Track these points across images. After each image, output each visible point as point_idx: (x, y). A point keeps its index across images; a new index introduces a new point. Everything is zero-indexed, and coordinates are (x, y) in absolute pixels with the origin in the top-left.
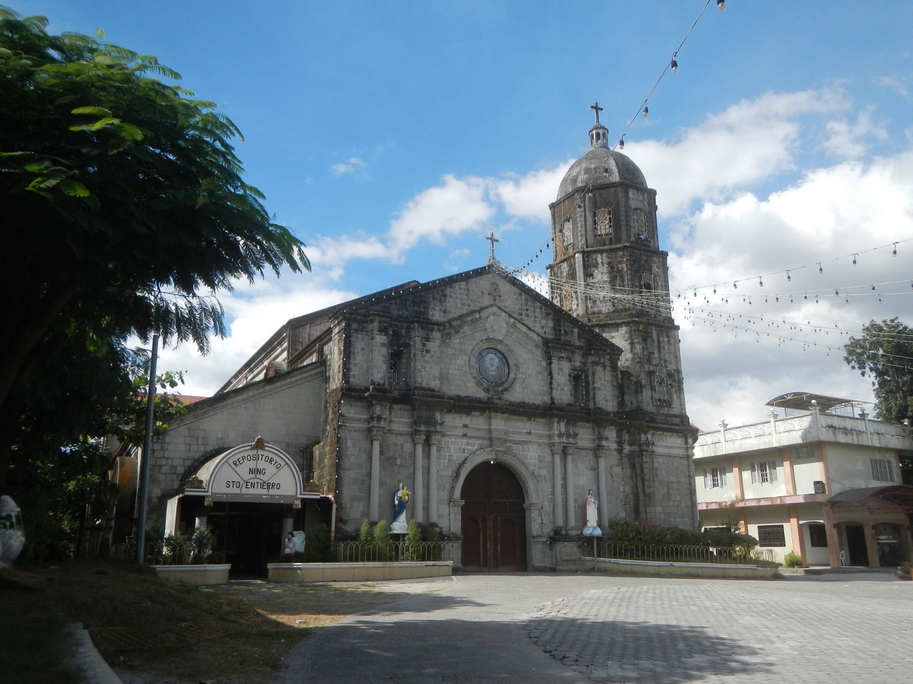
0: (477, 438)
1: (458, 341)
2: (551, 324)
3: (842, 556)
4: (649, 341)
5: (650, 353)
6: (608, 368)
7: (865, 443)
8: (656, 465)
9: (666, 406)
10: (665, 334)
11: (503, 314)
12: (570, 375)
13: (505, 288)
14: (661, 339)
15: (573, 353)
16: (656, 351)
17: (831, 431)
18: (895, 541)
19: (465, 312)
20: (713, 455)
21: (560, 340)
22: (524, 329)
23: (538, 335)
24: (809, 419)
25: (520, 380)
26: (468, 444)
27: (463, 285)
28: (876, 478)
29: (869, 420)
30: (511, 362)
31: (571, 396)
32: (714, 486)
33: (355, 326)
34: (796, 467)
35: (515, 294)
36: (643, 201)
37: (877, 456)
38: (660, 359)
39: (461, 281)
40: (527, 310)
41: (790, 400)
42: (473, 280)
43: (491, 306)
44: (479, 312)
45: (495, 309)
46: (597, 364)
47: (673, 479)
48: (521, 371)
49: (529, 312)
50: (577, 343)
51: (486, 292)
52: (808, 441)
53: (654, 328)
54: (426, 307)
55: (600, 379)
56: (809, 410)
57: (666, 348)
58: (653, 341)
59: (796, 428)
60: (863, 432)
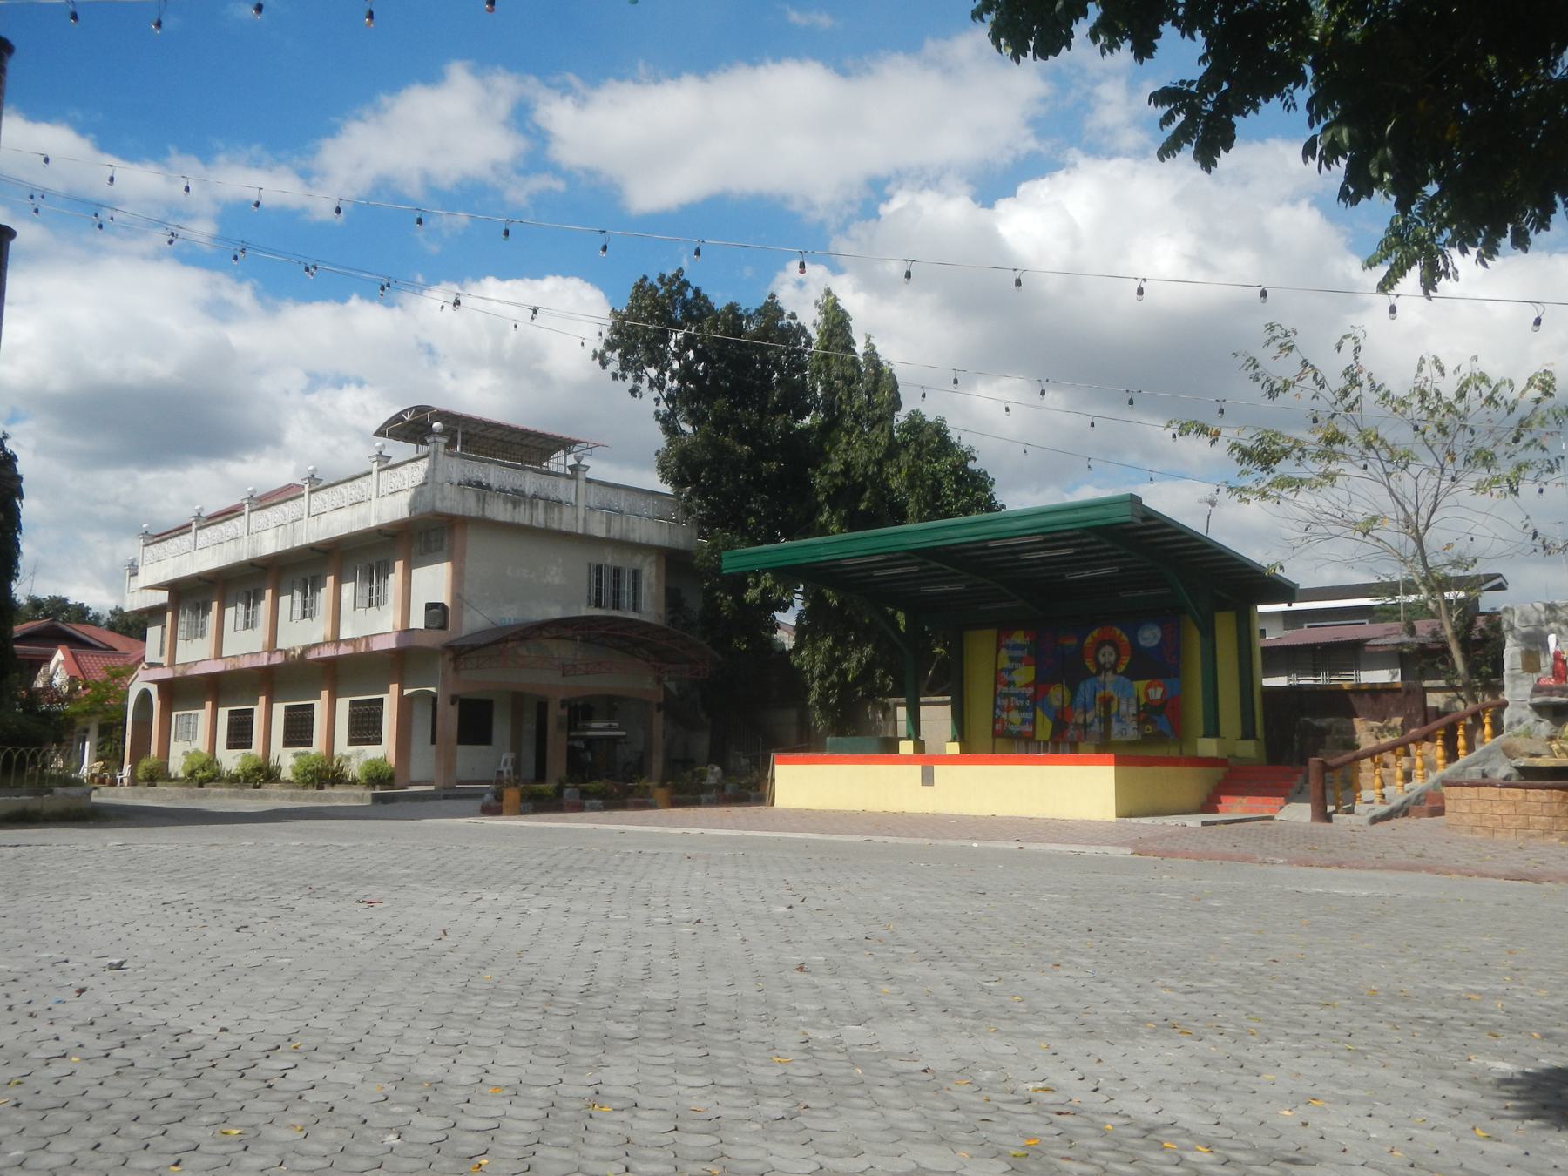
3: (505, 764)
7: (564, 528)
17: (471, 495)
18: (624, 733)
20: (288, 547)
24: (424, 464)
28: (598, 604)
29: (589, 481)
32: (304, 616)
34: (417, 574)
37: (610, 559)
41: (409, 422)
52: (418, 511)
56: (427, 444)
59: (406, 487)
60: (571, 504)
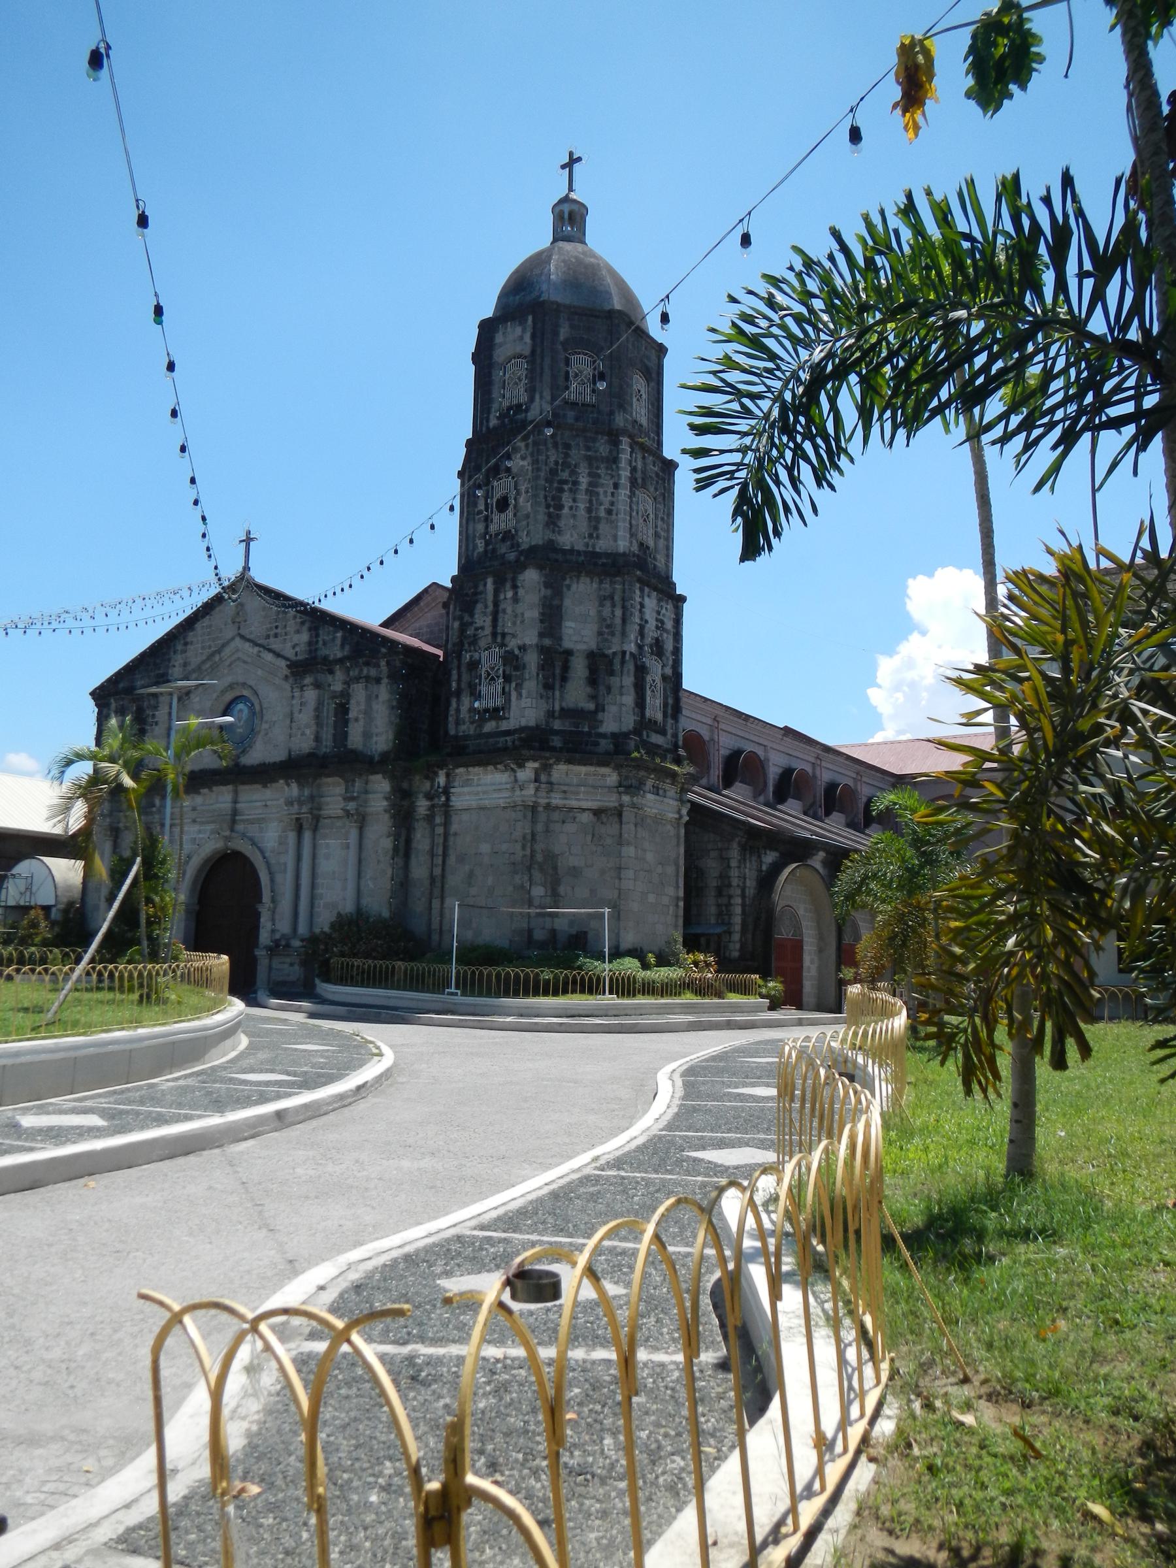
0: (208, 823)
1: (197, 699)
2: (305, 637)
4: (479, 606)
5: (477, 629)
6: (385, 681)
8: (454, 827)
9: (490, 719)
10: (508, 585)
11: (247, 644)
12: (317, 709)
13: (254, 603)
14: (502, 597)
15: (331, 672)
16: (489, 619)
19: (204, 658)
21: (315, 658)
22: (269, 657)
23: (286, 659)
25: (262, 733)
26: (200, 832)
27: (206, 622)
30: (257, 708)
31: (317, 739)
33: (105, 711)
35: (264, 609)
36: (521, 338)
38: (494, 634)
39: (203, 617)
40: (277, 627)
42: (217, 609)
43: (233, 639)
44: (219, 651)
45: (238, 639)
46: (357, 679)
47: (485, 848)
48: (265, 718)
49: (279, 631)
50: (339, 655)
51: (229, 621)
53: (490, 581)
54: (168, 667)
55: (358, 703)
57: (509, 610)
58: (486, 607)
